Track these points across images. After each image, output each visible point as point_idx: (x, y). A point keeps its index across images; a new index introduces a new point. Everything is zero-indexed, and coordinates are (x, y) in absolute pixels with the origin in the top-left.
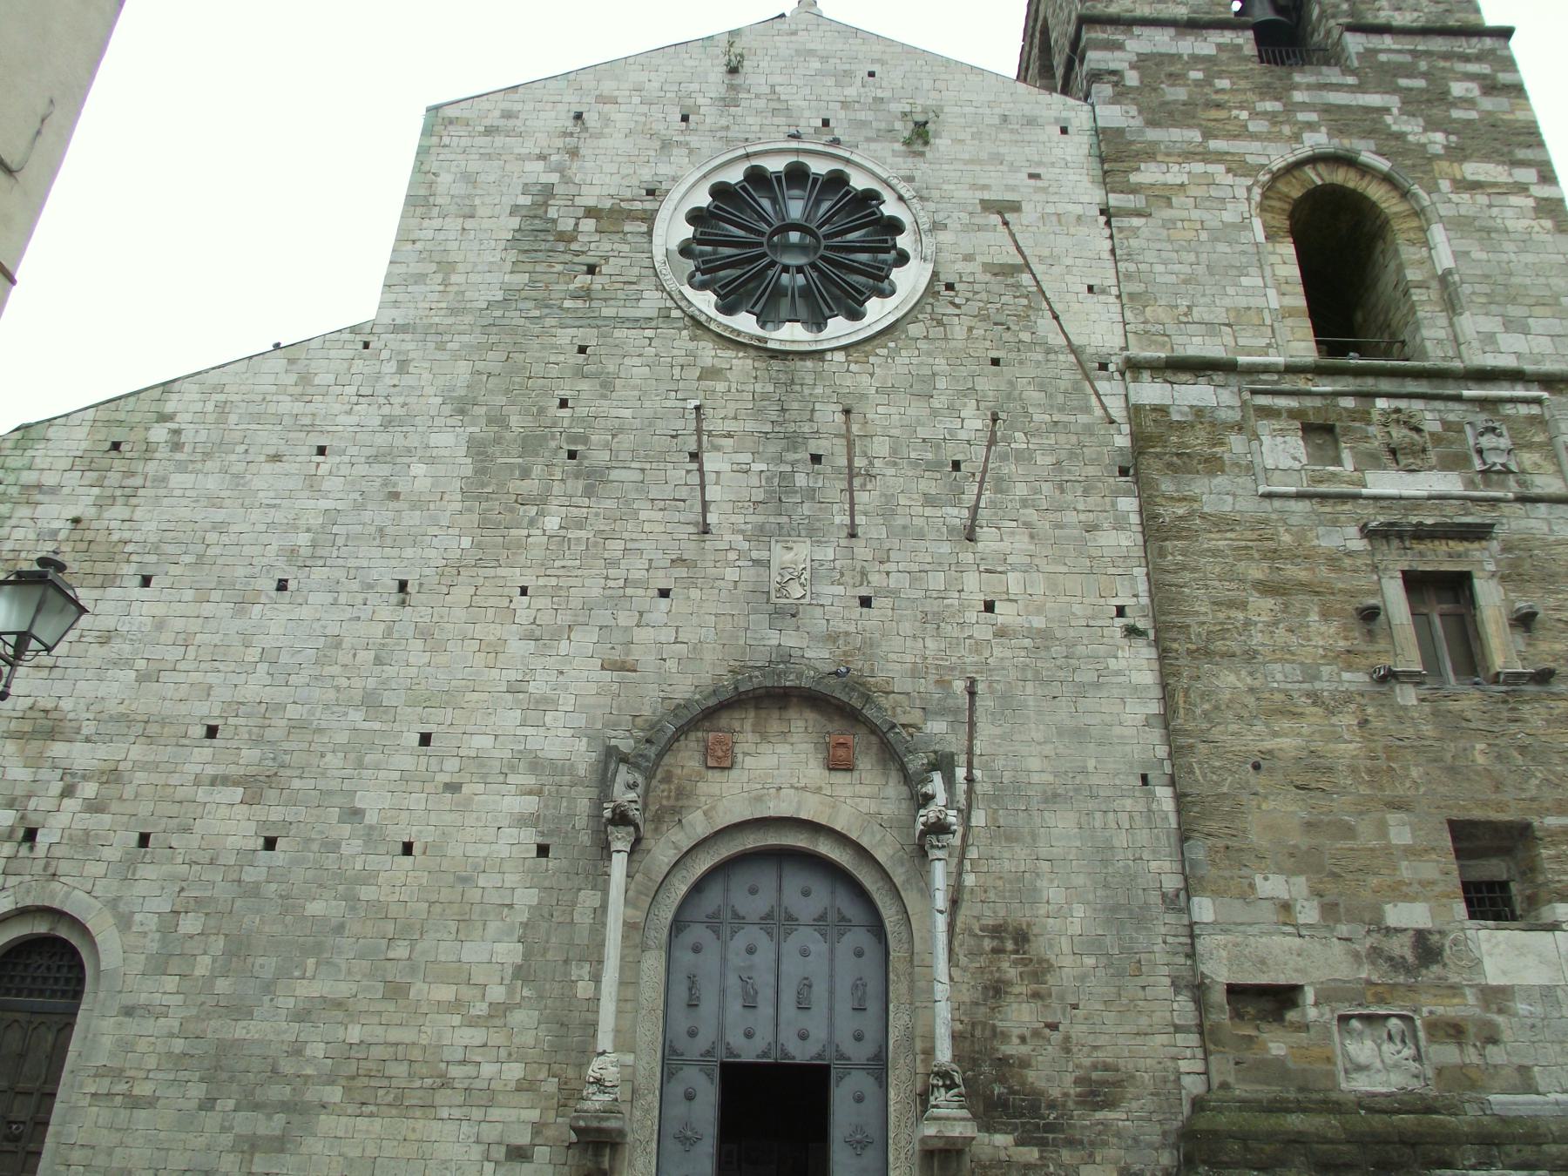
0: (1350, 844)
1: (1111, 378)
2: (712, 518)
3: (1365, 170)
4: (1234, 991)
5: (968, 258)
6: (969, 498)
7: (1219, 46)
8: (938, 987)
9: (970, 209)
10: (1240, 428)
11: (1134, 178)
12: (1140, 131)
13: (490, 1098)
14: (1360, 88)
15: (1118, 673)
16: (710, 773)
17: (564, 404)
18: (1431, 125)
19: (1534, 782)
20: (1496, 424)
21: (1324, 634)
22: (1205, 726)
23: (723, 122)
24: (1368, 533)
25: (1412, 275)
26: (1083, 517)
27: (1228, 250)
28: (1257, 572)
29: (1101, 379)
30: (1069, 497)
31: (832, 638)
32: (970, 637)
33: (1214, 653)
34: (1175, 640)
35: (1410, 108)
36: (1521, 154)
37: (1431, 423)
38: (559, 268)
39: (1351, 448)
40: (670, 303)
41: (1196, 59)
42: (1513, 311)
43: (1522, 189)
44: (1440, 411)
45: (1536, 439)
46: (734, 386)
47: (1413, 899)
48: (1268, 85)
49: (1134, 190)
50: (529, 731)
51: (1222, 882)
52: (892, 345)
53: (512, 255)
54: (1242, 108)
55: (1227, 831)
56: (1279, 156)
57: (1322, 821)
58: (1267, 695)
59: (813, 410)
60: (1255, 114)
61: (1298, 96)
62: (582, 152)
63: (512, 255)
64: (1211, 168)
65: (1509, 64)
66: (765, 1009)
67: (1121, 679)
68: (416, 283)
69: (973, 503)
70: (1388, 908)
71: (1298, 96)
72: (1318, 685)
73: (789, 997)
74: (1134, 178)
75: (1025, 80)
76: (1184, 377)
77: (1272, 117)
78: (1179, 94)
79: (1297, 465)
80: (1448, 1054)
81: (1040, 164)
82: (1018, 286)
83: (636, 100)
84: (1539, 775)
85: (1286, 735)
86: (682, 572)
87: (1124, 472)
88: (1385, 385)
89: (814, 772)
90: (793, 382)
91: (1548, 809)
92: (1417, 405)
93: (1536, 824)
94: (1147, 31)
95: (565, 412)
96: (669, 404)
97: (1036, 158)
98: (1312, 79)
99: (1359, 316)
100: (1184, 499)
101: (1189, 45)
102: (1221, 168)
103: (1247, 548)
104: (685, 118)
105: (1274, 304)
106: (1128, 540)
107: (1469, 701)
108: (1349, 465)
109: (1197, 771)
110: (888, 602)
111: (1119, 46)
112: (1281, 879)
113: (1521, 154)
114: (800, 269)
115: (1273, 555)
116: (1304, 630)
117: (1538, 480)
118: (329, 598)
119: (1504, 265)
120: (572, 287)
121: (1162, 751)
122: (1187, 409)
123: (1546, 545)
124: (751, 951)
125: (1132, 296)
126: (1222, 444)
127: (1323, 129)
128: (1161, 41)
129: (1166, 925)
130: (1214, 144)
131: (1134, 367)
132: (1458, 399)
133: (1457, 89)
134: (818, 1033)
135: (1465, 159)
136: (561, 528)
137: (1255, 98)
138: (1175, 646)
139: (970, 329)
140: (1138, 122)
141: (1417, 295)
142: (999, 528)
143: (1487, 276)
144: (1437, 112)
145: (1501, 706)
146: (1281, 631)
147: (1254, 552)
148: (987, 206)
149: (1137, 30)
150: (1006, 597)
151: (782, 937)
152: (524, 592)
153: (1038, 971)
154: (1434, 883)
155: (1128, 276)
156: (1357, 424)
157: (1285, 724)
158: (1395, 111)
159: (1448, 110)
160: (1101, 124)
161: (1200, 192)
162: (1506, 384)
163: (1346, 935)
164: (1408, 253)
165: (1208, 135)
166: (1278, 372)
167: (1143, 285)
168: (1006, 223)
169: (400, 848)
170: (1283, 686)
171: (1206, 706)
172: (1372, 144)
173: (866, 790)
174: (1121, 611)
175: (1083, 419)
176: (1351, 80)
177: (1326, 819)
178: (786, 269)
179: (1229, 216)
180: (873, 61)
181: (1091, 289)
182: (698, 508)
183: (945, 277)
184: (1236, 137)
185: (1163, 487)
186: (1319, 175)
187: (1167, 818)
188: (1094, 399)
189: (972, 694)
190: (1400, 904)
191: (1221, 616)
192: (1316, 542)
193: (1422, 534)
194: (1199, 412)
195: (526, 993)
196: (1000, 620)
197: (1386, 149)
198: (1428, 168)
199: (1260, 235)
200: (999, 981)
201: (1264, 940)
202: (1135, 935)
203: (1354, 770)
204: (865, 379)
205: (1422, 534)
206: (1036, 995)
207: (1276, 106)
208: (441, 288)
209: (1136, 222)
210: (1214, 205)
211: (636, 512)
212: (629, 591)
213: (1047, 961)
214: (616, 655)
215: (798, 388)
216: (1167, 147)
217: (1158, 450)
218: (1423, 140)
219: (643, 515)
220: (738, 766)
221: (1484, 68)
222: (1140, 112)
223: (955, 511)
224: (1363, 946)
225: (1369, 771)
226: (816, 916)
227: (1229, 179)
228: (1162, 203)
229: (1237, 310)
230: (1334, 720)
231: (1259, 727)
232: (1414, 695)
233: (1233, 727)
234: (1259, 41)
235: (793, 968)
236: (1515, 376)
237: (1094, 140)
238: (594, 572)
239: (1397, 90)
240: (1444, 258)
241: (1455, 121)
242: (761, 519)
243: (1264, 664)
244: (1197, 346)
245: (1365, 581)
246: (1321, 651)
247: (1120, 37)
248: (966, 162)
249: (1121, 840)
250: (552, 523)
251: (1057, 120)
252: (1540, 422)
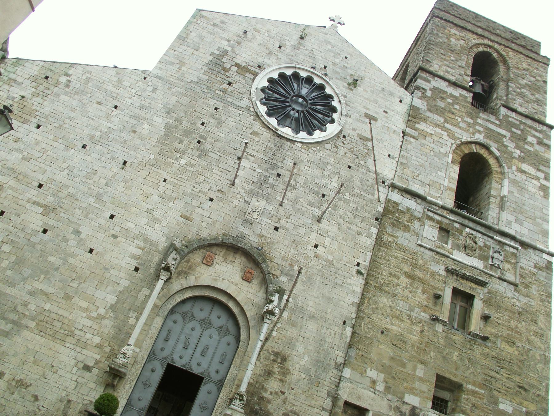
0: (403, 369)
1: (384, 187)
2: (237, 181)
3: (491, 153)
4: (346, 403)
5: (354, 130)
6: (324, 208)
8: (250, 365)
9: (361, 114)
10: (420, 220)
11: (417, 126)
12: (425, 112)
13: (85, 346)
14: (499, 126)
15: (349, 284)
16: (203, 265)
17: (203, 124)
18: (517, 147)
19: (469, 372)
20: (501, 251)
21: (421, 297)
22: (371, 312)
23: (292, 53)
24: (447, 270)
25: (493, 192)
26: (358, 229)
27: (438, 161)
28: (407, 269)
29: (381, 186)
30: (356, 221)
31: (261, 236)
32: (306, 254)
33: (383, 290)
34: (372, 281)
35: (512, 138)
36: (542, 168)
37: (481, 243)
38: (219, 79)
39: (452, 240)
40: (251, 105)
41: (451, 96)
42: (520, 217)
43: (538, 179)
44: (485, 240)
45: (512, 261)
46: (261, 141)
47: (416, 395)
48: (471, 113)
49: (416, 129)
50: (148, 228)
51: (356, 366)
52: (318, 148)
53: (205, 68)
54: (460, 117)
55: (364, 350)
56: (466, 137)
57: (396, 358)
58: (395, 310)
59: (284, 159)
60: (463, 121)
61: (479, 121)
62: (242, 44)
63: (205, 68)
64: (443, 132)
65: (549, 137)
66: (190, 351)
67: (350, 287)
68: (170, 65)
69: (324, 210)
70: (407, 395)
71: (479, 121)
72: (412, 313)
73: (199, 350)
74: (417, 126)
75: (395, 80)
76: (408, 196)
77: (468, 124)
78: (442, 104)
79: (433, 239)
81: (389, 109)
82: (366, 145)
83: (266, 34)
84: (471, 370)
85: (396, 326)
86: (220, 195)
87: (377, 219)
88: (471, 224)
89: (237, 278)
90: (281, 147)
91: (470, 382)
92: (479, 235)
93: (464, 386)
94: (439, 80)
95: (202, 127)
96: (238, 138)
97: (388, 106)
98: (485, 117)
99: (471, 199)
100: (393, 236)
101: (451, 90)
102: (446, 134)
103: (407, 260)
104: (280, 47)
105: (446, 184)
106: (370, 242)
107: (458, 337)
108: (450, 245)
109: (363, 327)
110: (283, 231)
111: (429, 81)
112: (376, 372)
113: (542, 168)
114: (298, 111)
115: (414, 265)
116: (415, 294)
117: (507, 274)
118: (99, 157)
119: (523, 201)
120: (221, 87)
121: (354, 315)
122: (405, 207)
123: (502, 296)
124: (193, 329)
125: (402, 163)
126: (412, 223)
127: (483, 135)
128: (443, 85)
129: (333, 373)
130: (447, 125)
131: (393, 186)
132: (492, 238)
133: (530, 139)
134: (205, 365)
135: (524, 162)
136: (186, 164)
137: (465, 116)
138: (371, 282)
139: (346, 153)
140: (425, 108)
141: (492, 199)
142: (329, 222)
143: (516, 202)
144: (521, 144)
145: (468, 343)
146: (407, 291)
147: (408, 262)
148: (367, 115)
149: (436, 78)
150: (323, 245)
151: (205, 329)
152: (165, 181)
153: (285, 372)
154: (424, 392)
155: (403, 156)
156: (457, 233)
157: (397, 322)
158: (508, 138)
159: (524, 144)
160: (413, 104)
161: (436, 139)
162: (509, 239)
163: (390, 399)
164: (494, 185)
165: (446, 121)
166: (439, 207)
167: (406, 161)
168: (370, 124)
169: (89, 250)
170: (401, 309)
171: (374, 306)
172: (496, 146)
173: (252, 291)
174: (358, 264)
175: (370, 197)
176: (498, 122)
177: (398, 358)
178: (293, 109)
179: (442, 150)
180: (348, 54)
181: (389, 156)
182: (234, 176)
183: (344, 133)
184: (455, 126)
185: (388, 229)
186: (476, 149)
187: (347, 338)
188: (376, 191)
189: (299, 273)
190: (411, 395)
191: (390, 279)
192: (429, 267)
193: (464, 277)
194: (408, 209)
195: (112, 315)
196: (318, 252)
197: (500, 149)
198: (511, 160)
199: (450, 160)
200: (271, 371)
201: (363, 390)
202: (321, 372)
203: (413, 346)
204: (305, 155)
205: (464, 277)
206: (281, 380)
207: (471, 121)
208: (178, 70)
209: (412, 140)
210: (439, 145)
211: (212, 169)
212: (200, 194)
213: (289, 370)
214: (187, 214)
215: (282, 150)
216: (431, 120)
217: (391, 216)
218: (513, 151)
219: (214, 171)
220: (213, 266)
221: (541, 136)
222: (427, 105)
223: (317, 210)
224: (394, 405)
225: (418, 348)
226: (219, 326)
227: (447, 138)
228: (423, 137)
229: (433, 181)
230: (413, 327)
231: (388, 320)
232: (441, 329)
233: (380, 317)
234: (474, 98)
235: (205, 340)
236: (513, 238)
237: (409, 108)
238: (191, 183)
239: (511, 131)
240: (505, 192)
241: (525, 149)
242: (253, 188)
243: (398, 300)
244: (416, 188)
245: (440, 285)
246: (417, 303)
247: (430, 79)
248: (366, 99)
249: (329, 340)
250: (183, 162)
251: (400, 97)
252: (515, 256)
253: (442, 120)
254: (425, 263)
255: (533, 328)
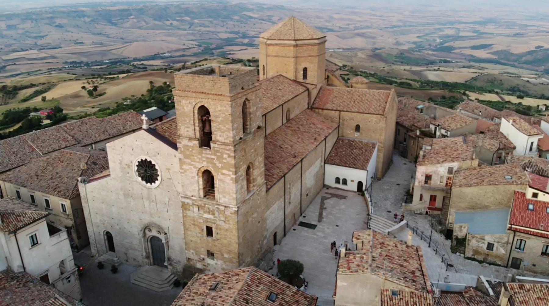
7: (194, 144)
10: (192, 206)
14: (211, 154)
21: (198, 230)
28: (192, 222)
43: (229, 175)
60: (198, 158)
74: (183, 167)
77: (199, 159)
80: (204, 267)
115: (194, 221)
130: (192, 163)
135: (223, 169)
148: (167, 169)
179: (193, 175)
194: (188, 203)
239: (216, 155)
253: (190, 161)
254: (197, 219)
255: (232, 234)
